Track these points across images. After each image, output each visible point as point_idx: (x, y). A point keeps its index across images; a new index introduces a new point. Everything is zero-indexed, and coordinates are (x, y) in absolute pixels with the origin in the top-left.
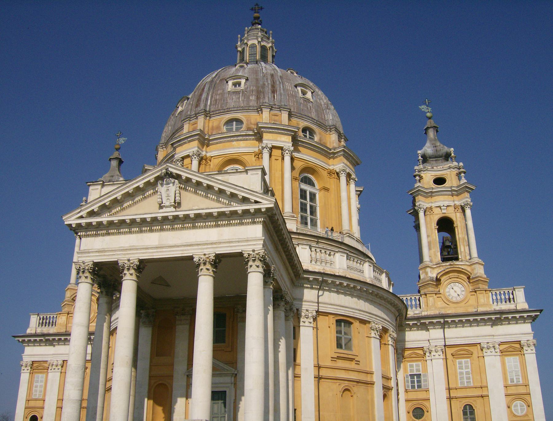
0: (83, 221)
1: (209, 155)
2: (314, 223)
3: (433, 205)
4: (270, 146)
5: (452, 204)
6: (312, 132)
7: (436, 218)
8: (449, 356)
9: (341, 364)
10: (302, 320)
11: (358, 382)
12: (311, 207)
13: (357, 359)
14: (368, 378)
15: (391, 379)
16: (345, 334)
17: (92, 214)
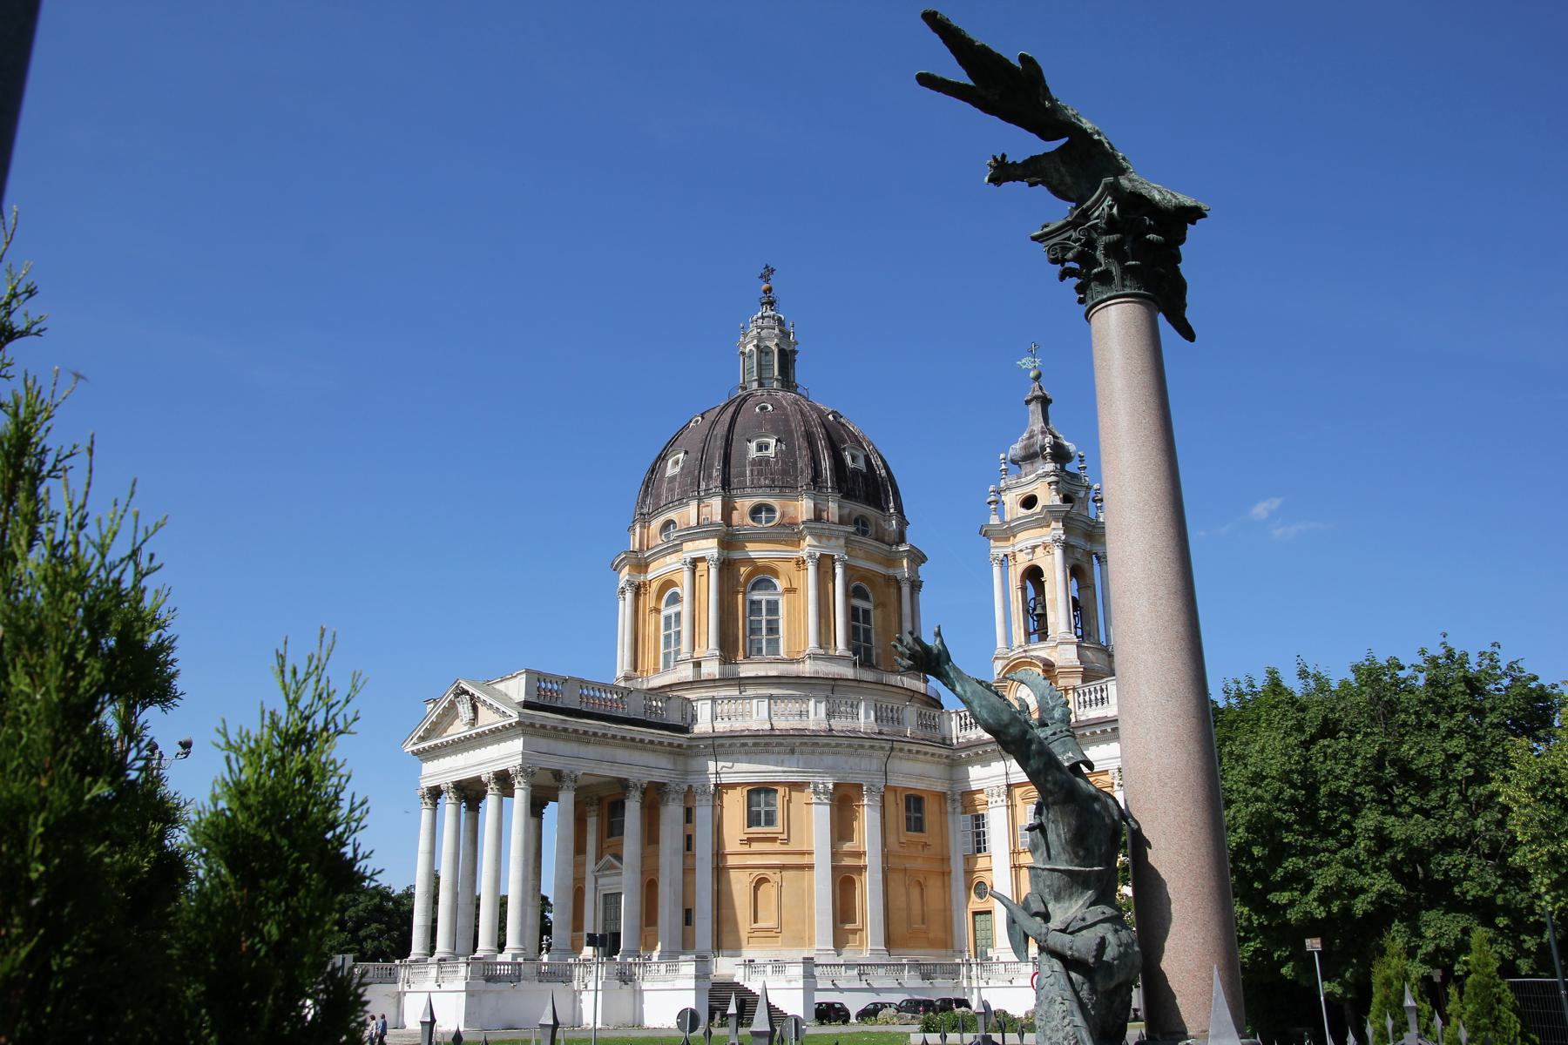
0: (415, 748)
1: (650, 577)
2: (773, 644)
3: (1017, 548)
4: (688, 560)
5: (1038, 541)
6: (770, 510)
7: (1020, 569)
8: (1018, 801)
9: (756, 846)
10: (697, 798)
11: (783, 867)
12: (768, 622)
13: (781, 836)
14: (805, 860)
15: (864, 853)
16: (767, 804)
17: (422, 739)
